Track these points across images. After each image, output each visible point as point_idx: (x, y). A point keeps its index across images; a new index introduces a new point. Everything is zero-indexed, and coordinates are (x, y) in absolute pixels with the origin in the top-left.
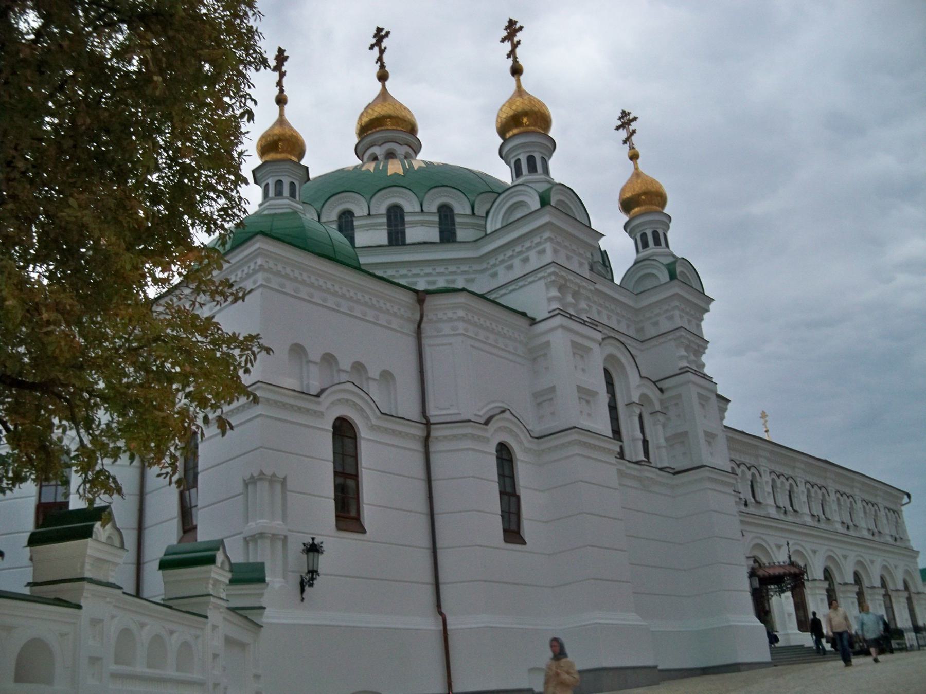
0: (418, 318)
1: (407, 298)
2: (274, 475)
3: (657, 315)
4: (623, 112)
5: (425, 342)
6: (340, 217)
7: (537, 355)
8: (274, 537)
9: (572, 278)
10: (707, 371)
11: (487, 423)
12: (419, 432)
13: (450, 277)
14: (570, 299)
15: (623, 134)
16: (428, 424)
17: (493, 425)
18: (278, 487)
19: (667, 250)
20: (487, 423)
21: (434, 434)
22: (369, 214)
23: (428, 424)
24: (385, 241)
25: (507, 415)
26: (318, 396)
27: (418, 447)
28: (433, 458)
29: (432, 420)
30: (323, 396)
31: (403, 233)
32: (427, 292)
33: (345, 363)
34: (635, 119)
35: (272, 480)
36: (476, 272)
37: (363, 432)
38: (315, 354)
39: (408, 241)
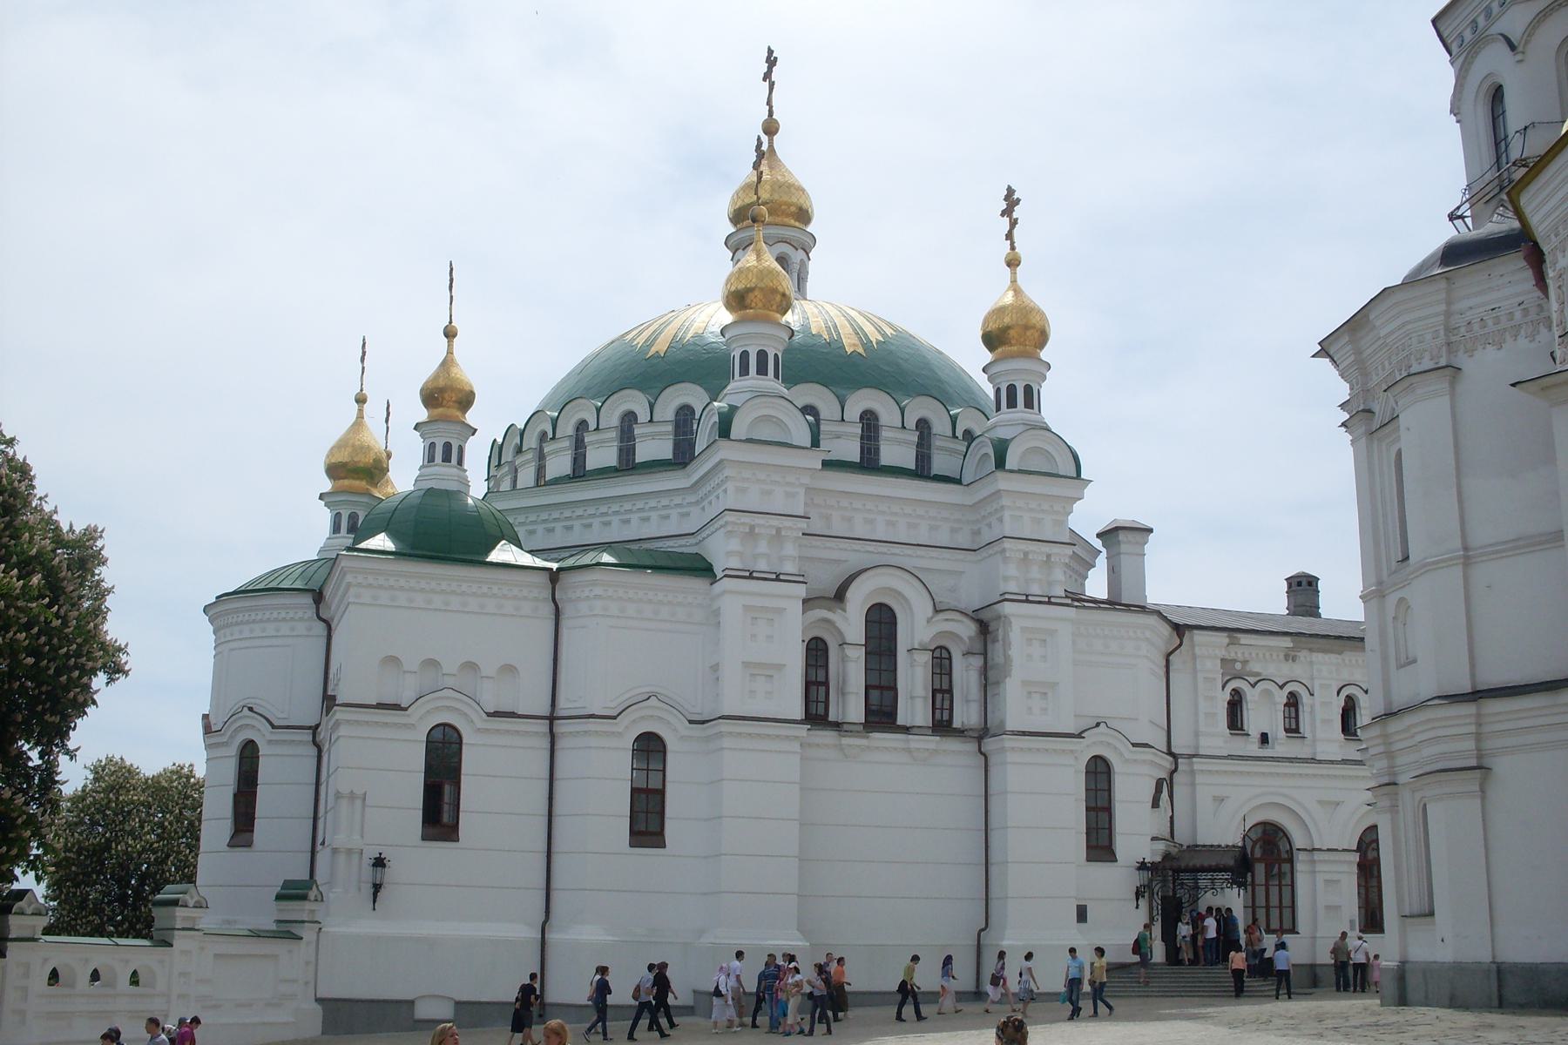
5: (564, 623)
8: (349, 851)
12: (543, 726)
13: (663, 512)
14: (763, 547)
17: (624, 720)
18: (358, 803)
19: (1028, 415)
22: (597, 429)
25: (653, 701)
26: (405, 709)
27: (546, 744)
28: (559, 755)
33: (450, 665)
34: (1018, 200)
35: (352, 796)
36: (690, 504)
39: (641, 456)
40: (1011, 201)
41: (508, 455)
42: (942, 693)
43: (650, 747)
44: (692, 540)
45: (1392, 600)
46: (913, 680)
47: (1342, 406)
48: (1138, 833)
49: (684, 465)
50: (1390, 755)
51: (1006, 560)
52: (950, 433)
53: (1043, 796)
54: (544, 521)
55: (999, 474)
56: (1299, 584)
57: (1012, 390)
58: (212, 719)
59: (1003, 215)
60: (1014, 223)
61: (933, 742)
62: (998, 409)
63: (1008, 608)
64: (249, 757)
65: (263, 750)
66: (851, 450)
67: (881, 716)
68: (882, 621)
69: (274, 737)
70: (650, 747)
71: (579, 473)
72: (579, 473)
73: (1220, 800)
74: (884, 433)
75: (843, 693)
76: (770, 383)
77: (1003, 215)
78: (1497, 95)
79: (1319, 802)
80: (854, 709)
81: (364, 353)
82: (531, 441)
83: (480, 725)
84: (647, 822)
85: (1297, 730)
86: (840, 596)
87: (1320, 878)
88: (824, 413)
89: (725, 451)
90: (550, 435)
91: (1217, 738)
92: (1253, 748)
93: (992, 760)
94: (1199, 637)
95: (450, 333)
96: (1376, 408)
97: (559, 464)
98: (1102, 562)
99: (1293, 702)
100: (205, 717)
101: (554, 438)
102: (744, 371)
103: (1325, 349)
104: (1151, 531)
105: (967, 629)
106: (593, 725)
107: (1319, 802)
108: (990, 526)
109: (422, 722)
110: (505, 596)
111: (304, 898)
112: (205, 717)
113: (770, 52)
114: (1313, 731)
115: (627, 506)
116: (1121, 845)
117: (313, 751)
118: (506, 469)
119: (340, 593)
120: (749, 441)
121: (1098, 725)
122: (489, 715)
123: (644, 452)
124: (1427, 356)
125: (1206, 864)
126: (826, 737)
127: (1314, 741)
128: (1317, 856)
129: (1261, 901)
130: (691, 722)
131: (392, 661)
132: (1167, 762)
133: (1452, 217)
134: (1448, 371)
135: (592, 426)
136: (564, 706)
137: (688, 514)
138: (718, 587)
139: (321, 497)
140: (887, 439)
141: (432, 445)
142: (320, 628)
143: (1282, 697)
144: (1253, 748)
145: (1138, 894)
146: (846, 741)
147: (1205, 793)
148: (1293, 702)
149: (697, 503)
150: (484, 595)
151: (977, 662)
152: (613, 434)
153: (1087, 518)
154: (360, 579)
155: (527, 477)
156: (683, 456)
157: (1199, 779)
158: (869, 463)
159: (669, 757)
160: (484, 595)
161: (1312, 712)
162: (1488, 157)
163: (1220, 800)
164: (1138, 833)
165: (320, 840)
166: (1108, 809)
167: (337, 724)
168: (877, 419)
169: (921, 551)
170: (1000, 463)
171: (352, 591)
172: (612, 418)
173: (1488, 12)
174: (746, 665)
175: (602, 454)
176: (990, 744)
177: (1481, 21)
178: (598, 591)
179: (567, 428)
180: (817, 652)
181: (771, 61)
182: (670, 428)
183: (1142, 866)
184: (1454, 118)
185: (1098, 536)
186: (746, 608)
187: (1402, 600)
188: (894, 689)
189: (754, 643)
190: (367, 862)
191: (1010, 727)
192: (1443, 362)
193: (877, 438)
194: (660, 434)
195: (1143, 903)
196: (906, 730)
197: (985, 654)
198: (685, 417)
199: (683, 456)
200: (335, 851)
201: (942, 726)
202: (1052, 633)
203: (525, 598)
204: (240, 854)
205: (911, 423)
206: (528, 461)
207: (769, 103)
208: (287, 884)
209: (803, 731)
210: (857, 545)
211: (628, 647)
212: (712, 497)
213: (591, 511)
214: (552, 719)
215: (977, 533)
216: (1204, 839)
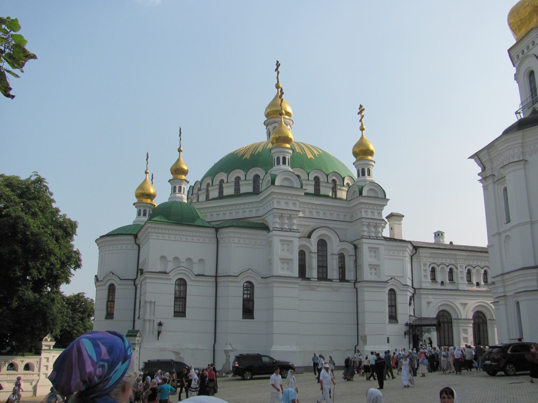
1: (213, 230)
2: (151, 301)
4: (361, 105)
5: (219, 245)
7: (270, 244)
8: (150, 320)
9: (285, 212)
12: (213, 279)
15: (359, 117)
18: (153, 304)
19: (368, 178)
22: (227, 182)
23: (216, 277)
25: (250, 271)
26: (168, 273)
27: (214, 285)
32: (219, 228)
33: (183, 259)
35: (151, 302)
36: (259, 207)
37: (188, 283)
38: (170, 258)
39: (241, 192)
40: (361, 110)
41: (195, 191)
42: (342, 269)
43: (250, 287)
44: (260, 218)
45: (504, 236)
46: (333, 265)
47: (479, 174)
48: (405, 314)
49: (258, 194)
50: (504, 286)
51: (363, 225)
52: (342, 184)
53: (375, 303)
54: (210, 212)
55: (360, 197)
56: (438, 235)
57: (363, 170)
58: (98, 277)
59: (358, 114)
60: (363, 117)
61: (339, 284)
62: (358, 176)
63: (364, 240)
64: (112, 289)
65: (117, 287)
66: (311, 189)
67: (323, 277)
68: (322, 244)
69: (122, 283)
70: (250, 287)
71: (221, 197)
72: (221, 197)
73: (429, 303)
74: (321, 184)
75: (311, 269)
76: (287, 167)
77: (358, 114)
78: (532, 73)
79: (461, 304)
80: (314, 274)
81: (148, 157)
82: (204, 186)
83: (193, 279)
84: (248, 311)
85: (452, 280)
86: (309, 236)
87: (461, 329)
88: (302, 177)
89: (273, 189)
90: (211, 184)
91: (427, 283)
92: (439, 286)
93: (359, 290)
94: (421, 250)
95: (180, 151)
96: (496, 174)
97: (214, 193)
98: (387, 226)
99: (451, 271)
100: (96, 276)
101: (212, 185)
102: (278, 163)
103: (477, 156)
104: (403, 216)
105: (350, 248)
106: (230, 279)
107: (461, 304)
108: (357, 214)
109: (174, 277)
110: (200, 236)
111: (136, 336)
112: (96, 276)
113: (278, 62)
114: (458, 280)
115: (238, 207)
116: (399, 317)
117: (134, 287)
118: (195, 195)
119: (144, 235)
120: (281, 186)
121: (392, 279)
122: (195, 275)
123: (243, 190)
124: (516, 156)
125: (425, 323)
126: (305, 282)
127: (458, 283)
128: (460, 321)
129: (442, 336)
130: (262, 278)
131: (163, 258)
132: (412, 291)
133: (517, 113)
134: (523, 162)
135: (225, 181)
136: (220, 273)
137: (259, 210)
138: (271, 233)
139: (134, 204)
140: (323, 186)
141: (175, 187)
142: (136, 247)
143: (448, 270)
144: (439, 286)
145: (405, 334)
146: (312, 284)
147: (424, 302)
148: (451, 271)
149: (262, 206)
150: (194, 236)
151: (354, 258)
152: (233, 184)
153: (385, 213)
154: (153, 230)
155: (203, 198)
156: (256, 191)
157: (422, 296)
158: (317, 194)
159: (255, 289)
160: (194, 236)
161: (457, 275)
162: (529, 94)
163: (429, 303)
164: (405, 314)
165: (137, 316)
166: (395, 306)
167: (146, 278)
168: (319, 179)
169: (334, 222)
170: (361, 193)
171: (150, 234)
172: (232, 178)
173: (528, 48)
174: (281, 259)
175: (229, 190)
176: (358, 285)
177: (526, 51)
178: (232, 235)
179: (217, 182)
180: (302, 254)
181: (278, 65)
182: (252, 182)
183: (407, 324)
184: (516, 82)
185: (386, 218)
186: (281, 240)
187: (507, 236)
188: (326, 267)
189: (283, 252)
190: (156, 324)
191: (365, 279)
192: (521, 159)
193: (319, 186)
195: (407, 337)
196: (331, 280)
197: (356, 255)
198: (256, 178)
199: (256, 191)
200: (145, 320)
201: (343, 279)
202: (378, 248)
203: (207, 237)
204: (109, 321)
205: (330, 181)
206: (204, 193)
207: (277, 78)
208: (129, 331)
209: (299, 281)
210: (314, 220)
211: (240, 253)
212: (268, 204)
213: (226, 209)
214: (216, 277)
215: (352, 216)
216: (424, 316)
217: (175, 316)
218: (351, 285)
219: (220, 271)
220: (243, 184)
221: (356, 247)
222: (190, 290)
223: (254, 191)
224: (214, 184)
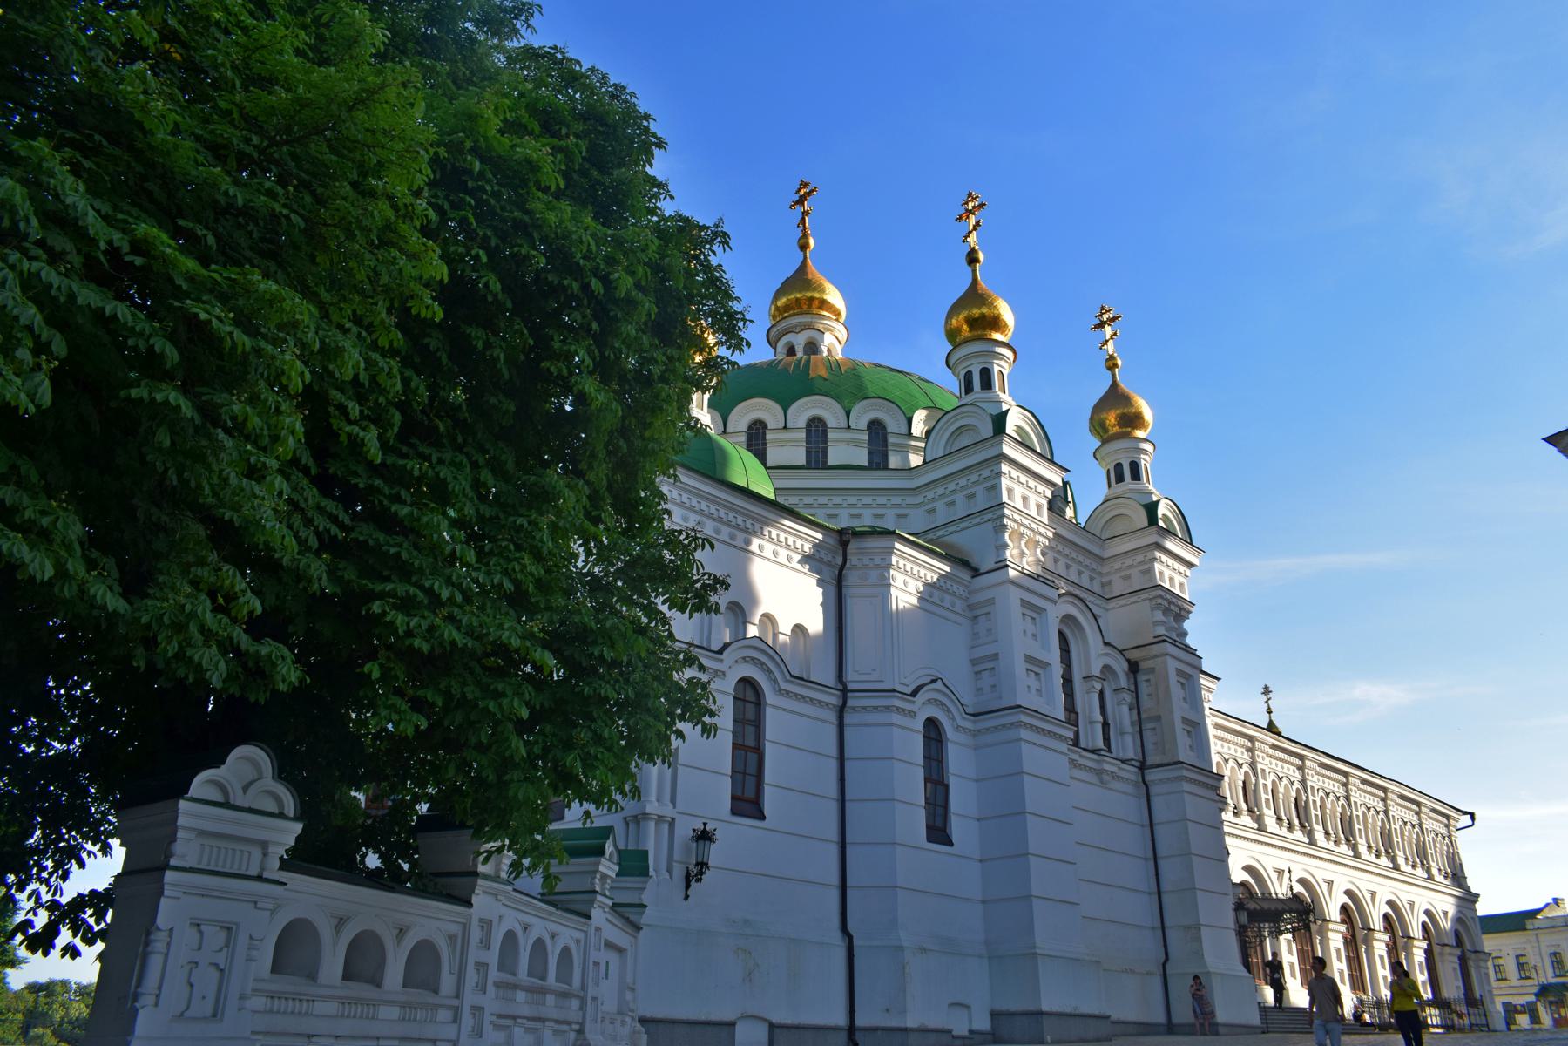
0: (840, 561)
3: (1131, 567)
6: (750, 428)
10: (1189, 641)
11: (914, 693)
12: (833, 699)
16: (844, 692)
17: (922, 696)
20: (914, 693)
21: (850, 703)
23: (844, 692)
24: (802, 461)
25: (938, 685)
26: (720, 652)
27: (832, 717)
28: (848, 732)
29: (850, 686)
30: (726, 653)
31: (825, 452)
36: (909, 506)
37: (770, 697)
39: (830, 462)
83: (784, 685)
105: (1121, 666)
115: (837, 500)
151: (1128, 697)
176: (1151, 775)
186: (1024, 603)
194: (854, 440)
217: (734, 812)
218: (1130, 773)
219: (851, 676)
220: (837, 440)
221: (1134, 668)
222: (775, 724)
223: (870, 462)
224: (729, 429)
